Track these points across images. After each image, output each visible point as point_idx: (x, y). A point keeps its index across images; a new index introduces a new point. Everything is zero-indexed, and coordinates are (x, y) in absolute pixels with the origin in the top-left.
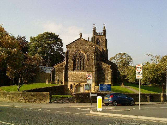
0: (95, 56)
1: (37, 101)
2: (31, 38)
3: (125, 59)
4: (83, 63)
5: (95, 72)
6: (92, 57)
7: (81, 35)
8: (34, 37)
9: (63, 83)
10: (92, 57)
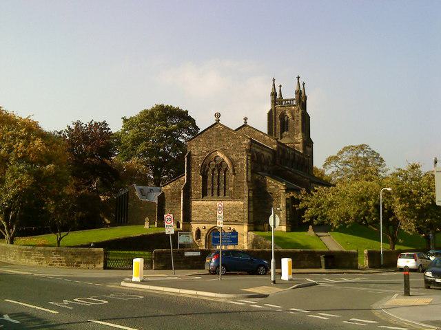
0: (249, 164)
1: (82, 266)
2: (125, 120)
3: (366, 160)
4: (223, 179)
5: (249, 200)
6: (242, 165)
7: (218, 115)
8: (131, 118)
10: (242, 165)
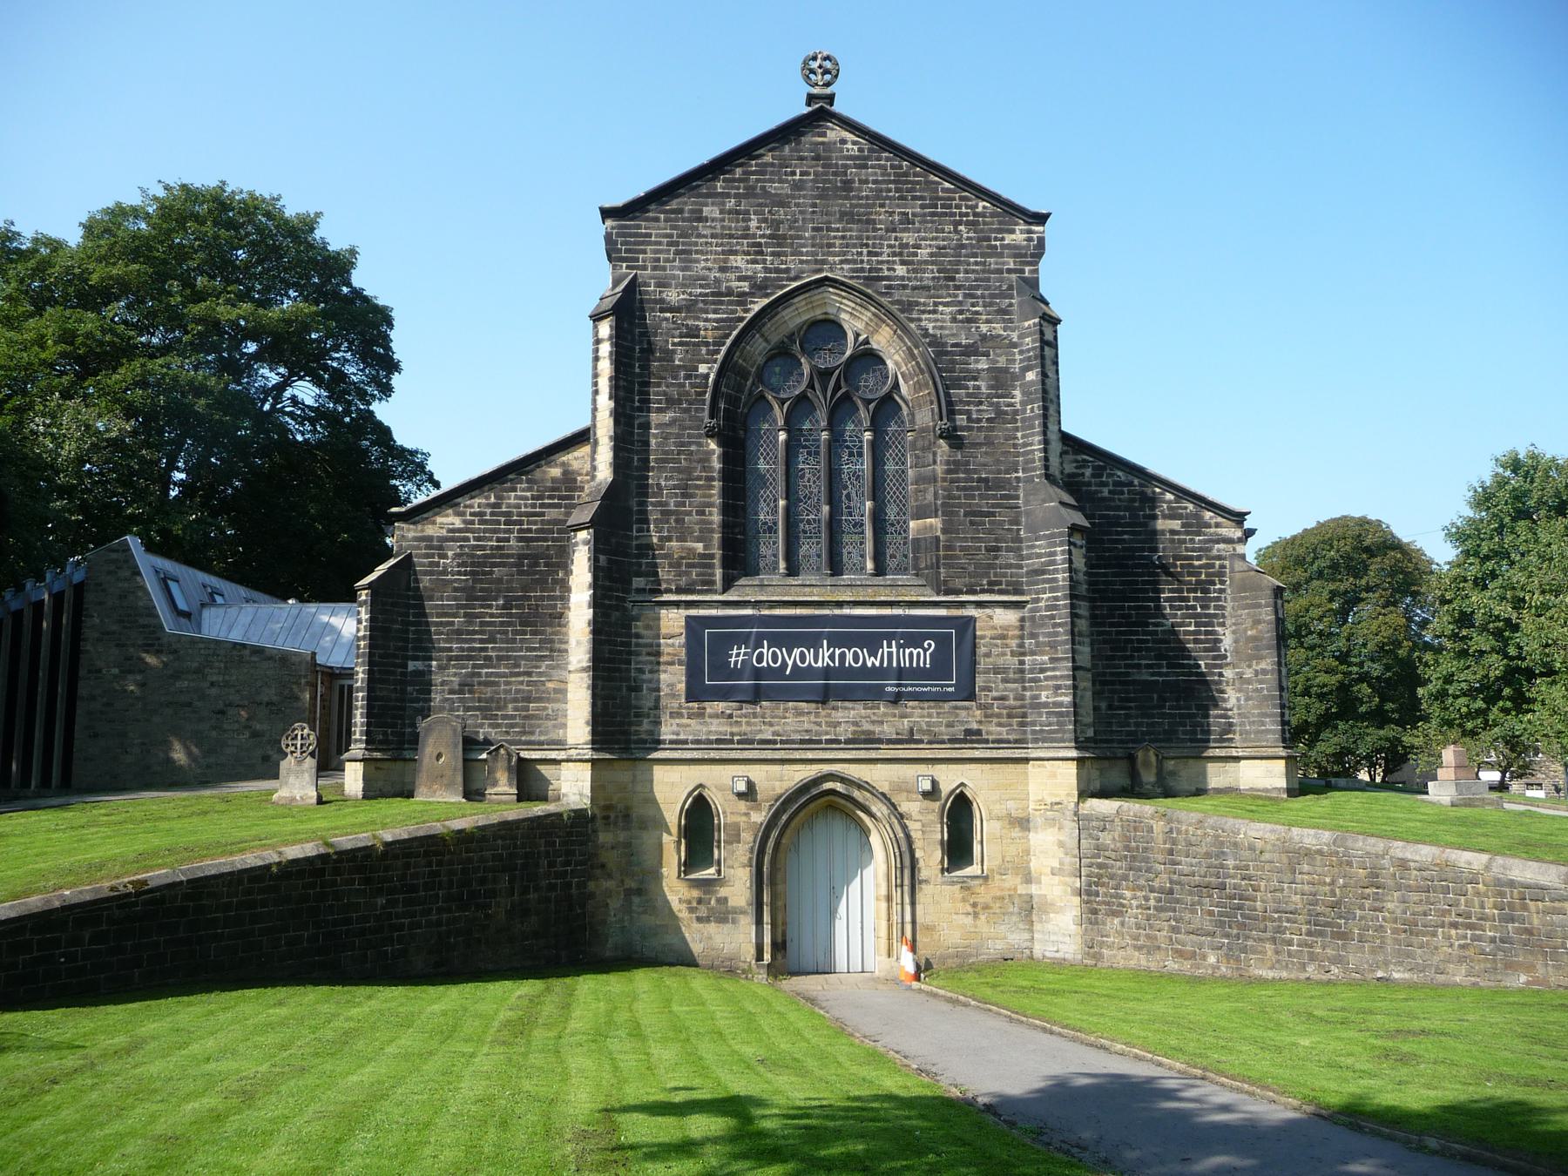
4: (866, 465)
7: (821, 69)
9: (573, 786)
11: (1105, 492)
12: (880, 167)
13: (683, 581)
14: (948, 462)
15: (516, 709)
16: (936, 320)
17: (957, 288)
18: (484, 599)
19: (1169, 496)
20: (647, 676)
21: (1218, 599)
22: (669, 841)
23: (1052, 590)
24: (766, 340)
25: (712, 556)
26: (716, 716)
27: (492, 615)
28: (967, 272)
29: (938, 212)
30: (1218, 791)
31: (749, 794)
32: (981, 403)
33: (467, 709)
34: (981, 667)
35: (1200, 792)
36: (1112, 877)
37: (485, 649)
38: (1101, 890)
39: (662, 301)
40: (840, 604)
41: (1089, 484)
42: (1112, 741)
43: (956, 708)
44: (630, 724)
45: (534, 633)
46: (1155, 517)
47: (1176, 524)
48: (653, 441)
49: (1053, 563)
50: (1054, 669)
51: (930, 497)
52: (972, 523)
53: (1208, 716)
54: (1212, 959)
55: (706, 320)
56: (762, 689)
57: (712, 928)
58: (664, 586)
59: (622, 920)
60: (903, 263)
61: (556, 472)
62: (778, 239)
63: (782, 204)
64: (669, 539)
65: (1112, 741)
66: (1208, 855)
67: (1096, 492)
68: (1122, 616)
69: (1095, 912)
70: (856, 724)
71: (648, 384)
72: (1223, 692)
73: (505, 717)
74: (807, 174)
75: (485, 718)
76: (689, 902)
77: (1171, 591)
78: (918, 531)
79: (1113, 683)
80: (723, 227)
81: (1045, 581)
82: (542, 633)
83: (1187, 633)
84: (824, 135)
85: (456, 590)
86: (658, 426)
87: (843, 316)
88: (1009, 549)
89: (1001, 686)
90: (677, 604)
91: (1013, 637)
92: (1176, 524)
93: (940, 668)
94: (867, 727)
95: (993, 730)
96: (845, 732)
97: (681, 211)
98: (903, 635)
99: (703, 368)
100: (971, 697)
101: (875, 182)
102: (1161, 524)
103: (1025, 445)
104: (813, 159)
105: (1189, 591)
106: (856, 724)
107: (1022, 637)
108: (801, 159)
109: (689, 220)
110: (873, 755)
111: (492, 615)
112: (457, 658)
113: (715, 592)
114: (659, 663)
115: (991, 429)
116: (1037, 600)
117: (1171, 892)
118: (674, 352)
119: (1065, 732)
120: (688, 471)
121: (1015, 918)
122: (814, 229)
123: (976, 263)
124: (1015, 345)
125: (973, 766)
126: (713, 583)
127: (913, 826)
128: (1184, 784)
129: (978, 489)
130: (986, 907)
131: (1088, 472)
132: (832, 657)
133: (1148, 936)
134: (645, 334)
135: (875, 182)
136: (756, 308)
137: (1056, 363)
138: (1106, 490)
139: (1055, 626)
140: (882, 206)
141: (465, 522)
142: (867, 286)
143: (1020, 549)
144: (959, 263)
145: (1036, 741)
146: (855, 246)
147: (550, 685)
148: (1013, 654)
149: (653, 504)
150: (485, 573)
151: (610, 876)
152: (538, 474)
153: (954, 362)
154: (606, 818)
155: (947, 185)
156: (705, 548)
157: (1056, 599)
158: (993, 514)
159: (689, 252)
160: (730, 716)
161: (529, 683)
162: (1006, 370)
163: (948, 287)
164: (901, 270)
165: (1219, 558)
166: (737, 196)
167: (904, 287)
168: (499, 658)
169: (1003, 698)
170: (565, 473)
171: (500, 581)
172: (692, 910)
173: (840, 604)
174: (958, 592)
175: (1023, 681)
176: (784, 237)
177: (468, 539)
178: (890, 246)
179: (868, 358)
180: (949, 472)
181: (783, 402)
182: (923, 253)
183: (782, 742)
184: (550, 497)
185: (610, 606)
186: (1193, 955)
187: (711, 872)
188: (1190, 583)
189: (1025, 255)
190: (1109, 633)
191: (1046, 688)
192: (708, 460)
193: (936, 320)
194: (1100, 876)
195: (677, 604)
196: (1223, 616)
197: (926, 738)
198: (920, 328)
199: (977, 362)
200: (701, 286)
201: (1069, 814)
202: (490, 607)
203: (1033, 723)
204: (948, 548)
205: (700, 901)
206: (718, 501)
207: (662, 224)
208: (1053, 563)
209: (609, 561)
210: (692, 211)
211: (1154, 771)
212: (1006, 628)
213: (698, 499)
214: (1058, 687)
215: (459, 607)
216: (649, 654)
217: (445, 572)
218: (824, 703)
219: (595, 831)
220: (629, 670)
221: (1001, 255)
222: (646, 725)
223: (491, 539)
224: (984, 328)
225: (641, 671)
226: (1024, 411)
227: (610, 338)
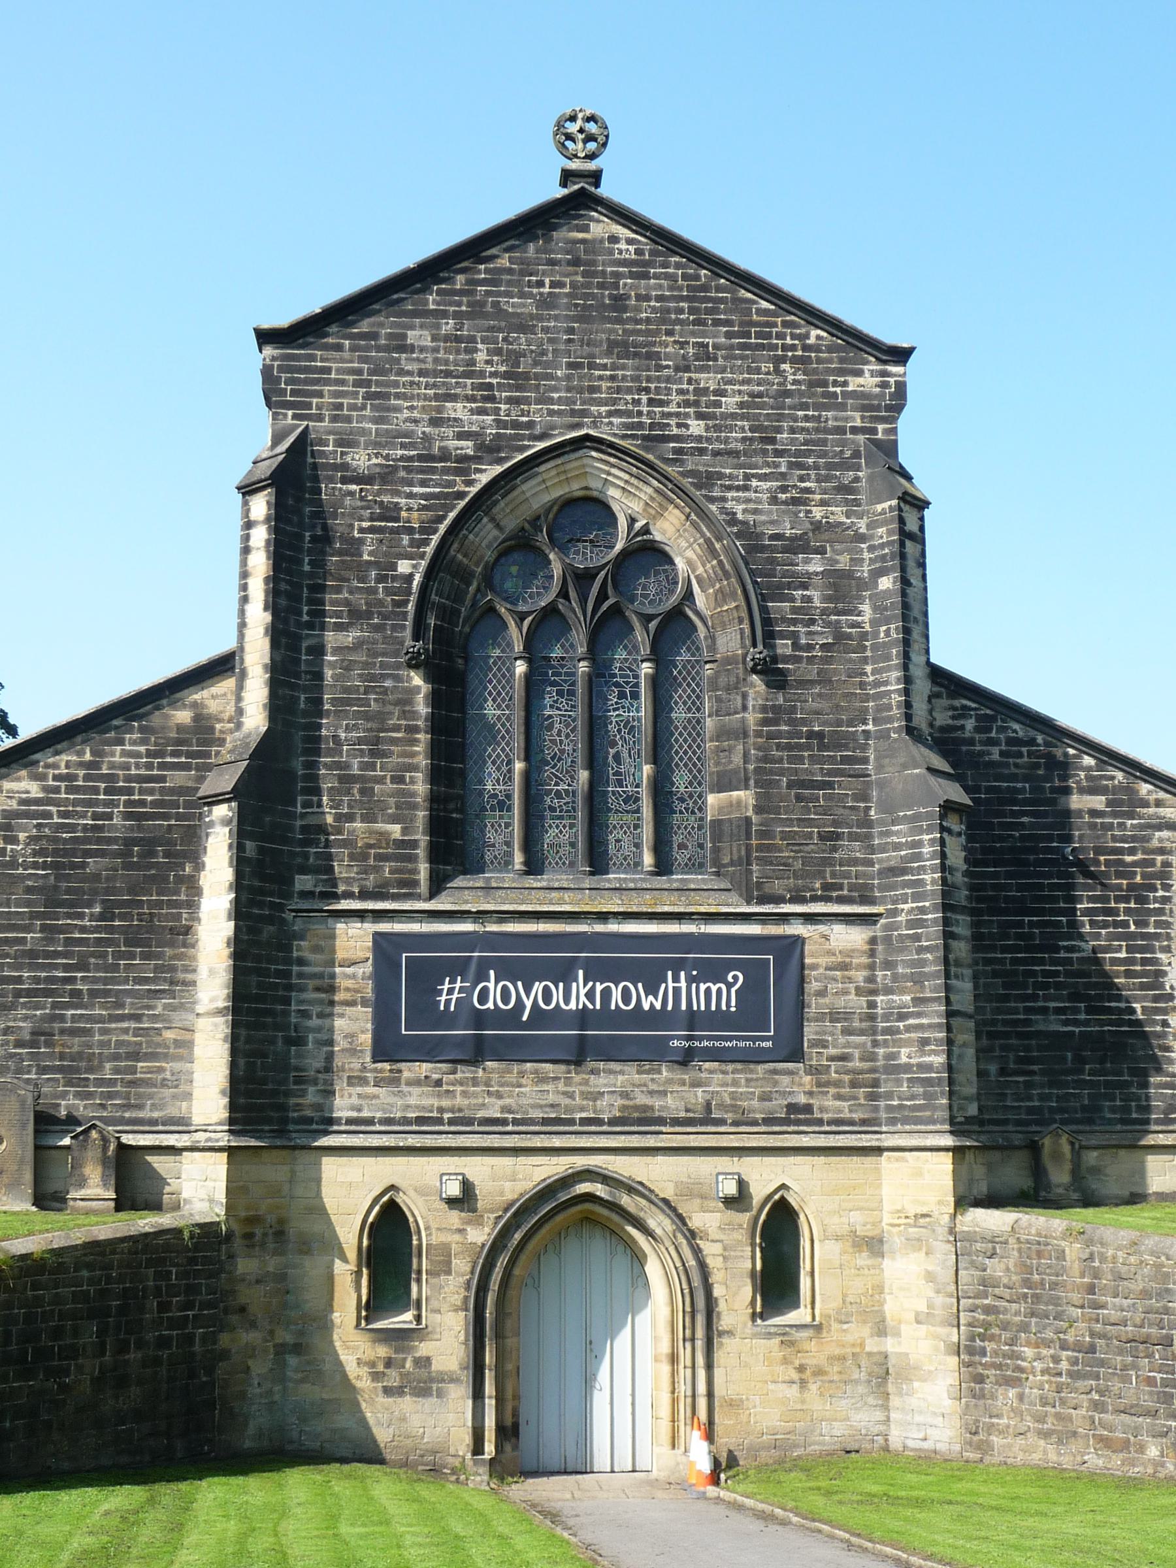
4: (643, 710)
7: (582, 133)
9: (199, 1188)
11: (995, 754)
12: (667, 276)
13: (371, 881)
14: (764, 709)
15: (116, 1071)
16: (748, 501)
17: (779, 453)
18: (72, 904)
19: (1088, 761)
20: (315, 1022)
21: (1160, 912)
22: (343, 1271)
23: (917, 897)
24: (498, 526)
25: (414, 844)
26: (417, 1082)
27: (83, 929)
28: (792, 430)
29: (751, 343)
30: (1163, 1197)
31: (465, 1200)
32: (812, 622)
33: (43, 1070)
34: (812, 1010)
35: (1136, 1198)
36: (1005, 1326)
37: (72, 980)
38: (990, 1346)
39: (345, 467)
40: (603, 917)
41: (971, 742)
42: (1005, 1122)
43: (775, 1072)
44: (288, 1094)
45: (146, 956)
46: (1067, 791)
47: (1098, 802)
48: (328, 673)
49: (918, 857)
50: (919, 1015)
51: (737, 759)
52: (799, 798)
53: (1145, 1085)
54: (1153, 1452)
55: (410, 496)
56: (486, 1042)
57: (407, 1403)
58: (342, 888)
59: (270, 1392)
60: (700, 416)
61: (183, 716)
62: (517, 379)
63: (524, 328)
64: (350, 818)
65: (1005, 1122)
66: (1145, 1294)
67: (982, 754)
68: (1019, 937)
69: (980, 1379)
70: (625, 1095)
71: (322, 588)
72: (1168, 1049)
73: (100, 1082)
74: (561, 285)
75: (69, 1083)
76: (372, 1364)
77: (1091, 899)
78: (720, 809)
79: (1006, 1035)
80: (436, 361)
81: (907, 884)
82: (158, 956)
83: (1114, 961)
84: (586, 229)
85: (29, 890)
86: (337, 650)
87: (612, 492)
88: (853, 837)
89: (842, 1040)
90: (361, 915)
91: (859, 967)
92: (1098, 802)
93: (750, 1012)
94: (642, 1099)
95: (830, 1105)
96: (609, 1107)
97: (374, 336)
98: (696, 963)
99: (404, 567)
100: (796, 1055)
101: (659, 298)
102: (1077, 801)
103: (877, 684)
104: (569, 263)
105: (1118, 899)
106: (625, 1095)
107: (872, 967)
108: (552, 262)
109: (387, 349)
110: (651, 1142)
111: (83, 929)
112: (29, 993)
113: (418, 897)
114: (332, 1003)
115: (827, 660)
116: (894, 913)
117: (1092, 1349)
118: (361, 541)
119: (935, 1108)
120: (381, 717)
121: (861, 1389)
122: (570, 366)
123: (807, 418)
124: (862, 538)
125: (799, 1159)
126: (415, 883)
127: (708, 1248)
128: (1112, 1188)
129: (808, 747)
130: (819, 1372)
131: (970, 724)
132: (590, 995)
133: (1058, 1416)
134: (319, 515)
135: (659, 298)
136: (484, 479)
137: (922, 565)
138: (995, 751)
139: (921, 949)
140: (670, 333)
141: (45, 789)
142: (647, 449)
143: (869, 836)
144: (780, 418)
145: (892, 1121)
146: (629, 391)
147: (169, 1035)
148: (859, 991)
149: (327, 766)
150: (74, 866)
151: (253, 1325)
152: (156, 719)
153: (772, 561)
154: (249, 1236)
155: (765, 305)
156: (405, 831)
157: (922, 910)
158: (830, 785)
159: (386, 396)
160: (439, 1083)
161: (137, 1032)
162: (848, 575)
163: (765, 452)
164: (696, 427)
165: (1162, 851)
166: (457, 315)
167: (702, 451)
168: (93, 993)
169: (843, 1058)
170: (198, 718)
171: (96, 877)
172: (376, 1376)
173: (603, 917)
174: (778, 900)
175: (874, 1031)
176: (526, 376)
177: (48, 815)
178: (681, 392)
179: (647, 554)
180: (765, 722)
181: (522, 617)
182: (730, 403)
183: (516, 1122)
184: (174, 754)
185: (261, 918)
186: (1125, 1445)
187: (405, 1319)
188: (1119, 887)
189: (877, 408)
190: (1001, 961)
191: (907, 1043)
192: (409, 702)
193: (748, 501)
194: (987, 1325)
195: (361, 915)
196: (1168, 937)
197: (729, 1117)
198: (723, 510)
199: (807, 561)
200: (403, 446)
201: (942, 1232)
202: (81, 916)
203: (889, 1095)
204: (763, 834)
205: (389, 1363)
206: (423, 761)
207: (346, 355)
208: (918, 857)
209: (261, 850)
210: (390, 336)
211: (1068, 1166)
212: (850, 953)
213: (394, 760)
214: (924, 1042)
215: (33, 916)
216: (318, 989)
217: (13, 864)
218: (578, 1063)
219: (231, 1256)
220: (286, 1013)
221: (842, 407)
222: (311, 1096)
223: (84, 816)
224: (818, 513)
225: (305, 1014)
226: (876, 634)
227: (268, 519)
